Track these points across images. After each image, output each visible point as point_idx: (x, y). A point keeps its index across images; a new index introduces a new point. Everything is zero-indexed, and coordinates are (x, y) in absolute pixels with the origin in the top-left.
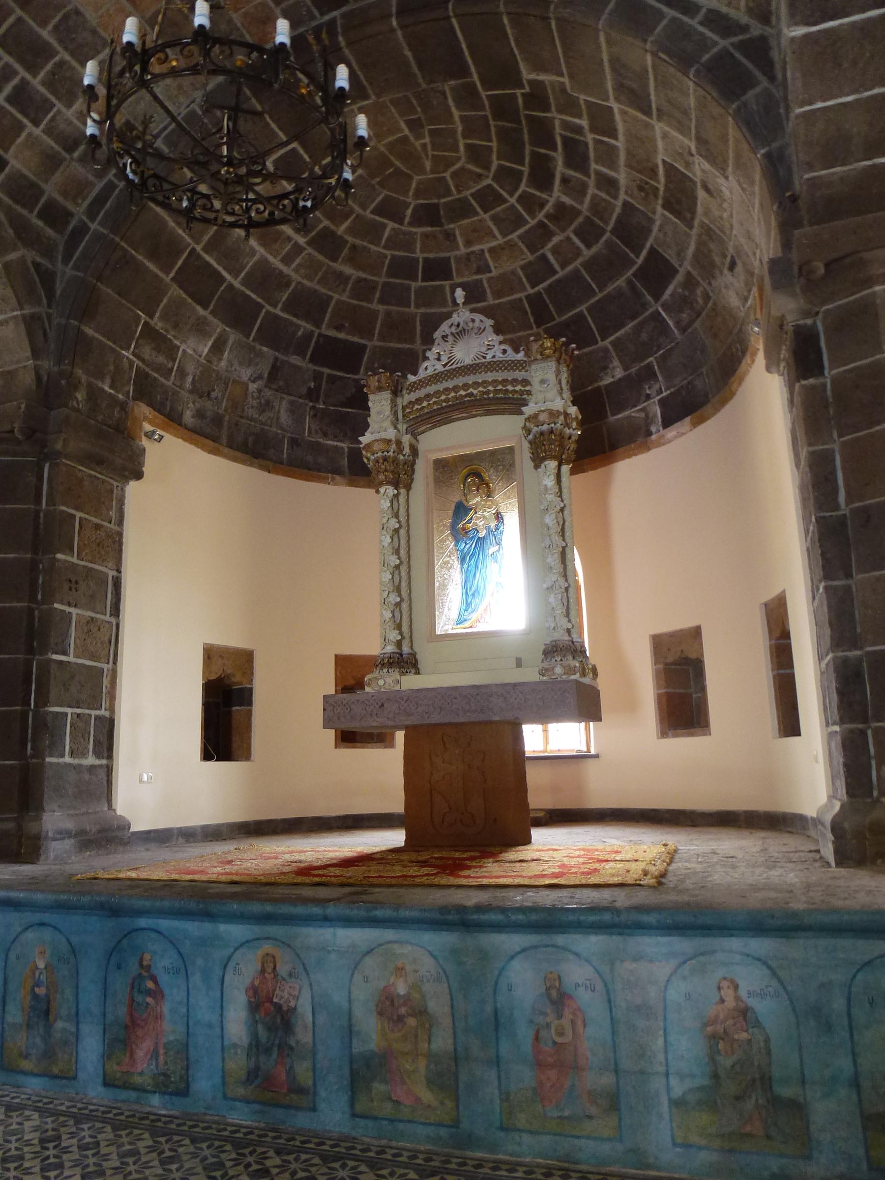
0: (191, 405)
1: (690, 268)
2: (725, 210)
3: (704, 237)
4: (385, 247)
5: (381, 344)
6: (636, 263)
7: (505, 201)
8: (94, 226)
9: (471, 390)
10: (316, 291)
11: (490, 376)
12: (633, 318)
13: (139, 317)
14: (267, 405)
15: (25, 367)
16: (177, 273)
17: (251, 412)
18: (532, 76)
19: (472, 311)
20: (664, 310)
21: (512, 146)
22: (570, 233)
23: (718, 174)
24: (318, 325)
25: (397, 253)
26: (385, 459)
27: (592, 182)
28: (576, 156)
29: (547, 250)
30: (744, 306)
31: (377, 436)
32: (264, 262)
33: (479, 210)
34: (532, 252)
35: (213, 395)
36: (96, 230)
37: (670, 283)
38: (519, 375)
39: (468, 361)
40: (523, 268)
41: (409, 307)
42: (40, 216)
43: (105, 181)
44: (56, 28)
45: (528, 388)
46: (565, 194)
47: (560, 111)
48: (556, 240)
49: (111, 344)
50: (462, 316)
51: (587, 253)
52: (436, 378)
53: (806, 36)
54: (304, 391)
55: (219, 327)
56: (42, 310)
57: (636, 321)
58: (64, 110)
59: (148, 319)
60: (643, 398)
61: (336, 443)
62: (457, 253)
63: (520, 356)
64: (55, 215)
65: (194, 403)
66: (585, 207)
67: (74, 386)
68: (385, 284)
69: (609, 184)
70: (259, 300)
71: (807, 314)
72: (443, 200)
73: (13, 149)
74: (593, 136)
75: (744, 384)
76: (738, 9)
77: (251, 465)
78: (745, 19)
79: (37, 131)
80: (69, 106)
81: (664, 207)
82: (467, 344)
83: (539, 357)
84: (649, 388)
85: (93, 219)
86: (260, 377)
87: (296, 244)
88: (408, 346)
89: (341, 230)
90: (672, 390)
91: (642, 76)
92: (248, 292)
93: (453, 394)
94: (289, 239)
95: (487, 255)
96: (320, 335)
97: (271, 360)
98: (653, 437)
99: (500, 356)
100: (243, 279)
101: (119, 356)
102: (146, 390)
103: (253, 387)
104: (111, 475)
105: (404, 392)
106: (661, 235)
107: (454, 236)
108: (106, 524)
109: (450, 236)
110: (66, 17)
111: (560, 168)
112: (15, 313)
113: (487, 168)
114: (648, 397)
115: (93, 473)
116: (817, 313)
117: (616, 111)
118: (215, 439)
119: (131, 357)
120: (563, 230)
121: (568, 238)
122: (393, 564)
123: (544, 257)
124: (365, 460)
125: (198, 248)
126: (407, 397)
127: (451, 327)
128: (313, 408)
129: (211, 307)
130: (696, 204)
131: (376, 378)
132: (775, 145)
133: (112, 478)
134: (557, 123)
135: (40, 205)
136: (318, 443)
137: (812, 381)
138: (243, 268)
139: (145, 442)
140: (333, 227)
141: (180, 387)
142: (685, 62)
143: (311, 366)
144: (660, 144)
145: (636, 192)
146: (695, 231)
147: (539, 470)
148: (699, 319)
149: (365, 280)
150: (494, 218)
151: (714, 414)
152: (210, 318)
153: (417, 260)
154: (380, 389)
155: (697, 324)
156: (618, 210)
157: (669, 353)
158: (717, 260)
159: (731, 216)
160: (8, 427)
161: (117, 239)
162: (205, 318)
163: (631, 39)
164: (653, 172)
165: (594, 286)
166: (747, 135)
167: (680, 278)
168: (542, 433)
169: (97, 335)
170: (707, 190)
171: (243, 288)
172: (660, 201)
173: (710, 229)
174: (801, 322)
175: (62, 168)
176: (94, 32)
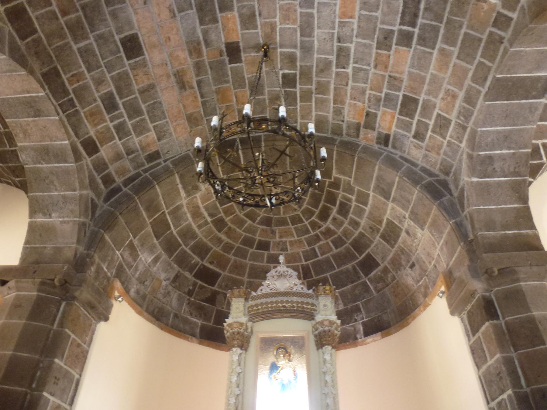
0: (135, 286)
1: (387, 265)
2: (415, 242)
3: (399, 252)
4: (243, 231)
5: (229, 274)
6: (358, 258)
7: (303, 222)
8: (124, 189)
9: (284, 304)
10: (206, 244)
11: (295, 299)
12: (352, 282)
13: (130, 236)
15: (70, 247)
16: (153, 220)
17: (160, 296)
18: (337, 176)
19: (287, 267)
20: (369, 281)
22: (329, 241)
23: (417, 227)
24: (202, 259)
25: (248, 235)
26: (238, 333)
27: (346, 222)
28: (344, 209)
29: (316, 247)
30: (417, 285)
31: (236, 320)
32: (190, 225)
33: (290, 224)
34: (309, 246)
35: (146, 283)
36: (126, 191)
37: (374, 270)
38: (310, 301)
40: (303, 252)
41: (246, 259)
42: (101, 178)
43: (136, 171)
44: (149, 106)
45: (314, 307)
46: (332, 224)
47: (343, 191)
48: (321, 243)
49: (113, 246)
50: (282, 268)
51: (335, 251)
52: (267, 295)
53: (478, 182)
54: (187, 290)
55: (160, 250)
56: (87, 221)
57: (353, 284)
58: (135, 137)
59: (133, 239)
60: (353, 320)
61: (195, 320)
62: (275, 240)
63: (311, 291)
64: (108, 180)
65: (136, 285)
66: (340, 232)
67: (92, 264)
68: (238, 247)
69: (356, 224)
70: (181, 242)
71: (487, 291)
72: (275, 216)
73: (105, 147)
74: (355, 203)
75: (416, 320)
76: (435, 168)
77: (154, 324)
78: (437, 172)
79: (119, 143)
80: (137, 137)
81: (381, 237)
82: (283, 281)
83: (323, 293)
84: (357, 316)
85: (125, 185)
86: (168, 279)
87: (206, 221)
88: (242, 278)
89: (227, 219)
90: (369, 318)
91: (391, 185)
92: (178, 237)
93: (275, 305)
94: (204, 218)
95: (288, 244)
96: (202, 264)
97: (176, 272)
98: (360, 340)
99: (301, 291)
100: (178, 230)
101: (114, 253)
102: (120, 273)
103: (164, 283)
104: (94, 316)
105: (250, 299)
106: (375, 248)
107: (275, 233)
108: (83, 344)
109: (273, 232)
110: (155, 103)
112: (75, 219)
113: (300, 207)
114: (356, 320)
115: (86, 313)
116: (492, 291)
117: (371, 195)
118: (141, 306)
119: (119, 255)
120: (326, 239)
121: (328, 243)
122: (236, 394)
123: (314, 249)
124: (225, 332)
125: (166, 212)
126: (251, 303)
127: (276, 272)
128: (188, 299)
129: (160, 240)
130: (399, 238)
131: (238, 290)
132: (458, 219)
133: (93, 318)
134: (340, 195)
135: (103, 174)
136: (187, 318)
137: (495, 322)
138: (180, 225)
139: (114, 302)
140: (224, 217)
141: (133, 276)
143: (194, 279)
144: (388, 212)
145: (368, 229)
146: (394, 249)
147: (320, 350)
148: (387, 288)
149: (230, 243)
150: (295, 228)
151: (395, 332)
152: (158, 245)
153: (255, 240)
154: (240, 296)
155: (386, 289)
156: (356, 235)
157: (368, 301)
158: (404, 263)
159: (418, 245)
160: (53, 277)
161: (136, 198)
162: (155, 244)
163: (391, 170)
164: (380, 222)
165: (335, 266)
166: (444, 212)
167: (380, 268)
168: (324, 331)
169: (109, 240)
170: (408, 233)
171: (176, 235)
172: (379, 235)
173: (403, 249)
174: (484, 294)
175: (121, 161)
176: (163, 112)
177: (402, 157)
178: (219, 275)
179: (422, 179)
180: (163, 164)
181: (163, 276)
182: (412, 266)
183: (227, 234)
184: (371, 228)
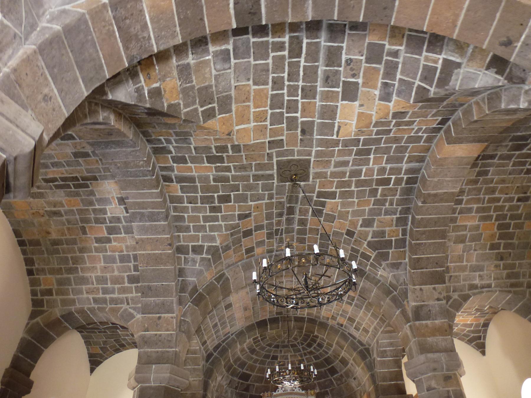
8: (215, 354)
14: (227, 392)
21: (305, 340)
22: (312, 356)
36: (216, 356)
39: (289, 391)
52: (281, 395)
63: (304, 392)
66: (318, 353)
69: (327, 353)
99: (299, 392)
103: (225, 387)
111: (315, 345)
132: (373, 372)
142: (355, 350)
143: (238, 380)
155: (342, 385)
157: (333, 389)
164: (339, 356)
177: (349, 333)
178: (251, 375)
179: (358, 347)
180: (232, 337)
181: (225, 383)
182: (355, 379)
183: (256, 355)
184: (334, 356)
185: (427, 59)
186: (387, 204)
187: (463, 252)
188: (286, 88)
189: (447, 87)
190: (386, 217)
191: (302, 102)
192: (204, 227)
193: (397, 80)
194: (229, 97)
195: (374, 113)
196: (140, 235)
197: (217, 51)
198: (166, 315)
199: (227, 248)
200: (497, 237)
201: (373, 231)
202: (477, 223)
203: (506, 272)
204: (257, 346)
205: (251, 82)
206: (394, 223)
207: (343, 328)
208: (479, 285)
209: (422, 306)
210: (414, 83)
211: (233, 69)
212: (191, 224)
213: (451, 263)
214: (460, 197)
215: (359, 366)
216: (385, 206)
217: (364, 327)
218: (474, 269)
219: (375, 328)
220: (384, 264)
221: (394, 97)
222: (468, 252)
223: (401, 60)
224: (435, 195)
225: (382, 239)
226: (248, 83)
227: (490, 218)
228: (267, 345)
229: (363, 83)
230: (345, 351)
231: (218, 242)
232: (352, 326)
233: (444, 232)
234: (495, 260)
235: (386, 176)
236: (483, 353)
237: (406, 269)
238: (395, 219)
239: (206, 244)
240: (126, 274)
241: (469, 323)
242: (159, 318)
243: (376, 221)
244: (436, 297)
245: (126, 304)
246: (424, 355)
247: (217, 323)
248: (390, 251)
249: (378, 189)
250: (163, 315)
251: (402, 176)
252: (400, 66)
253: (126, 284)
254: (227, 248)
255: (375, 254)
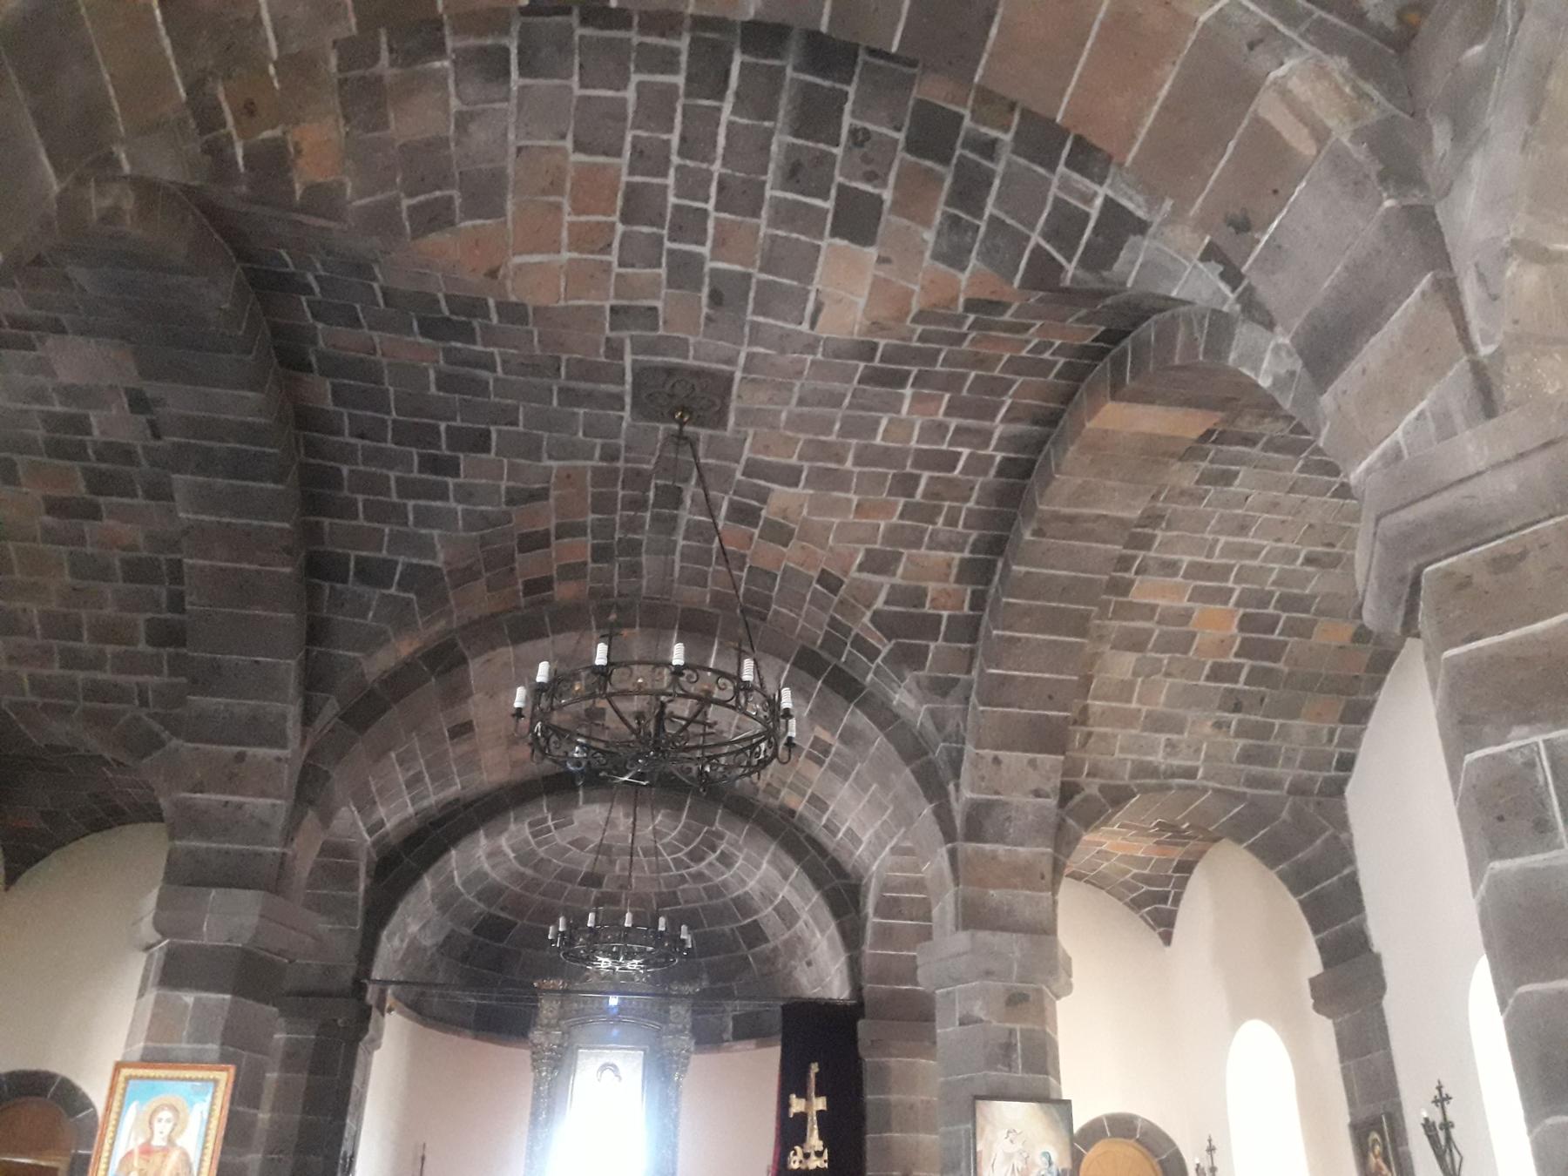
111: (712, 857)
164: (776, 896)
185: (1065, 185)
186: (941, 520)
187: (1135, 674)
188: (672, 172)
189: (1105, 274)
190: (933, 553)
191: (717, 219)
192: (399, 513)
193: (986, 217)
194: (498, 177)
195: (917, 288)
196: (196, 513)
197: (466, 50)
198: (262, 752)
199: (465, 576)
200: (1235, 649)
201: (893, 587)
202: (1185, 603)
203: (1241, 742)
204: (539, 844)
205: (568, 144)
206: (954, 571)
207: (795, 820)
208: (1163, 767)
209: (989, 805)
210: (1028, 238)
211: (514, 101)
212: (360, 498)
213: (1095, 698)
214: (1148, 531)
215: (822, 931)
216: (934, 523)
217: (849, 829)
218: (1158, 723)
219: (877, 835)
220: (910, 676)
221: (973, 261)
222: (1148, 676)
223: (1000, 168)
224: (1071, 519)
225: (912, 610)
226: (560, 143)
227: (1223, 595)
228: (572, 843)
229: (894, 203)
230: (791, 885)
231: (441, 556)
232: (820, 818)
233: (1085, 617)
234: (1220, 708)
235: (944, 447)
236: (1167, 939)
237: (967, 699)
238: (956, 562)
239: (401, 559)
240: (141, 619)
241: (1140, 854)
242: (240, 757)
243: (904, 559)
244: (1033, 787)
245: (137, 702)
246: (969, 933)
247: (421, 772)
248: (932, 645)
249: (918, 477)
250: (250, 751)
251: (989, 451)
252: (997, 182)
253: (142, 646)
254: (469, 574)
255: (890, 646)
